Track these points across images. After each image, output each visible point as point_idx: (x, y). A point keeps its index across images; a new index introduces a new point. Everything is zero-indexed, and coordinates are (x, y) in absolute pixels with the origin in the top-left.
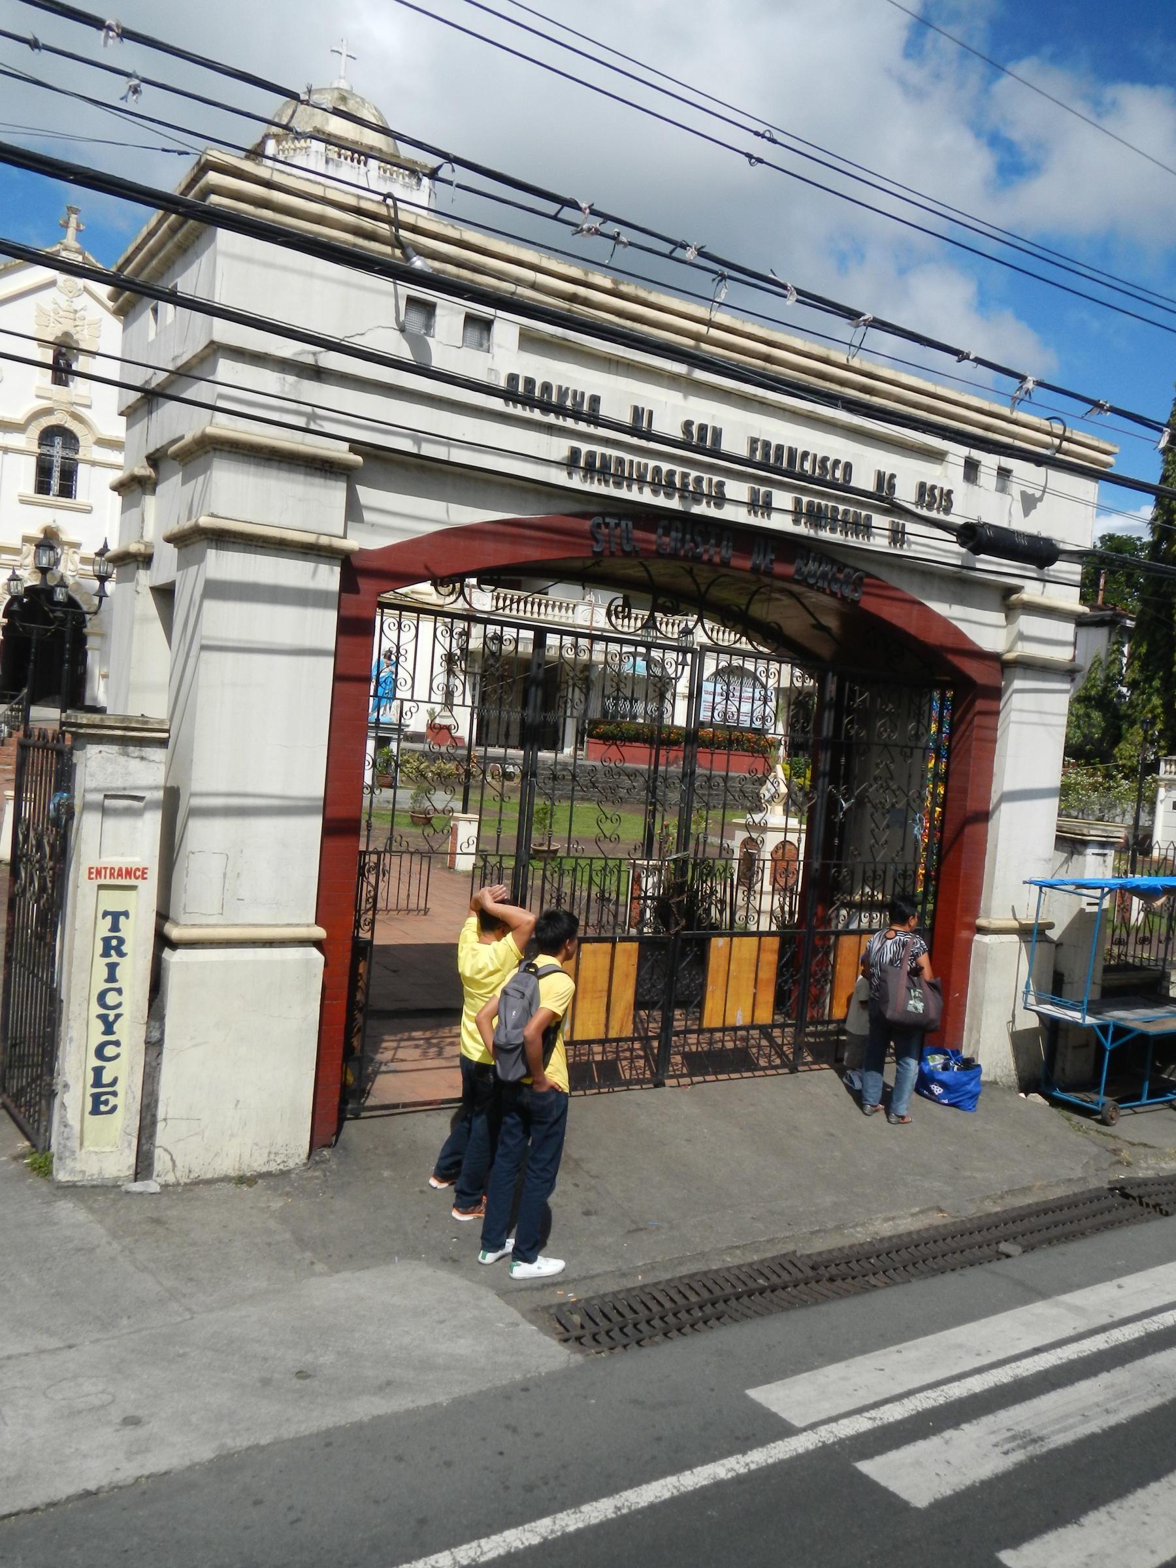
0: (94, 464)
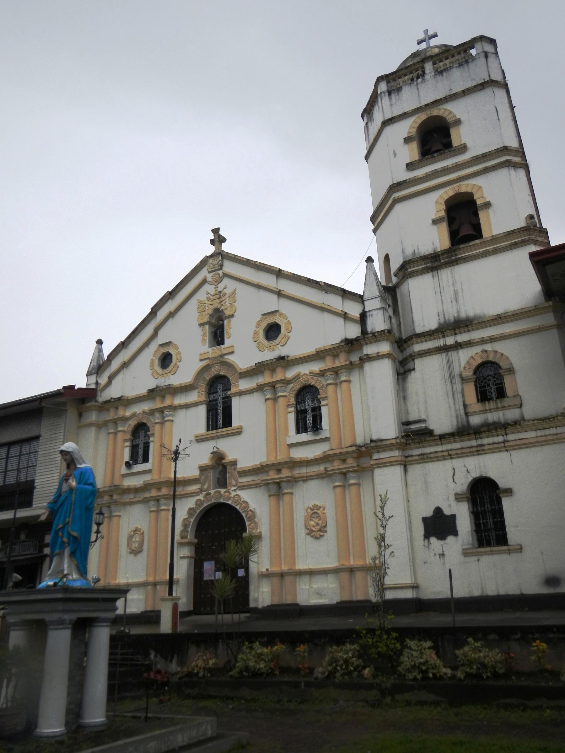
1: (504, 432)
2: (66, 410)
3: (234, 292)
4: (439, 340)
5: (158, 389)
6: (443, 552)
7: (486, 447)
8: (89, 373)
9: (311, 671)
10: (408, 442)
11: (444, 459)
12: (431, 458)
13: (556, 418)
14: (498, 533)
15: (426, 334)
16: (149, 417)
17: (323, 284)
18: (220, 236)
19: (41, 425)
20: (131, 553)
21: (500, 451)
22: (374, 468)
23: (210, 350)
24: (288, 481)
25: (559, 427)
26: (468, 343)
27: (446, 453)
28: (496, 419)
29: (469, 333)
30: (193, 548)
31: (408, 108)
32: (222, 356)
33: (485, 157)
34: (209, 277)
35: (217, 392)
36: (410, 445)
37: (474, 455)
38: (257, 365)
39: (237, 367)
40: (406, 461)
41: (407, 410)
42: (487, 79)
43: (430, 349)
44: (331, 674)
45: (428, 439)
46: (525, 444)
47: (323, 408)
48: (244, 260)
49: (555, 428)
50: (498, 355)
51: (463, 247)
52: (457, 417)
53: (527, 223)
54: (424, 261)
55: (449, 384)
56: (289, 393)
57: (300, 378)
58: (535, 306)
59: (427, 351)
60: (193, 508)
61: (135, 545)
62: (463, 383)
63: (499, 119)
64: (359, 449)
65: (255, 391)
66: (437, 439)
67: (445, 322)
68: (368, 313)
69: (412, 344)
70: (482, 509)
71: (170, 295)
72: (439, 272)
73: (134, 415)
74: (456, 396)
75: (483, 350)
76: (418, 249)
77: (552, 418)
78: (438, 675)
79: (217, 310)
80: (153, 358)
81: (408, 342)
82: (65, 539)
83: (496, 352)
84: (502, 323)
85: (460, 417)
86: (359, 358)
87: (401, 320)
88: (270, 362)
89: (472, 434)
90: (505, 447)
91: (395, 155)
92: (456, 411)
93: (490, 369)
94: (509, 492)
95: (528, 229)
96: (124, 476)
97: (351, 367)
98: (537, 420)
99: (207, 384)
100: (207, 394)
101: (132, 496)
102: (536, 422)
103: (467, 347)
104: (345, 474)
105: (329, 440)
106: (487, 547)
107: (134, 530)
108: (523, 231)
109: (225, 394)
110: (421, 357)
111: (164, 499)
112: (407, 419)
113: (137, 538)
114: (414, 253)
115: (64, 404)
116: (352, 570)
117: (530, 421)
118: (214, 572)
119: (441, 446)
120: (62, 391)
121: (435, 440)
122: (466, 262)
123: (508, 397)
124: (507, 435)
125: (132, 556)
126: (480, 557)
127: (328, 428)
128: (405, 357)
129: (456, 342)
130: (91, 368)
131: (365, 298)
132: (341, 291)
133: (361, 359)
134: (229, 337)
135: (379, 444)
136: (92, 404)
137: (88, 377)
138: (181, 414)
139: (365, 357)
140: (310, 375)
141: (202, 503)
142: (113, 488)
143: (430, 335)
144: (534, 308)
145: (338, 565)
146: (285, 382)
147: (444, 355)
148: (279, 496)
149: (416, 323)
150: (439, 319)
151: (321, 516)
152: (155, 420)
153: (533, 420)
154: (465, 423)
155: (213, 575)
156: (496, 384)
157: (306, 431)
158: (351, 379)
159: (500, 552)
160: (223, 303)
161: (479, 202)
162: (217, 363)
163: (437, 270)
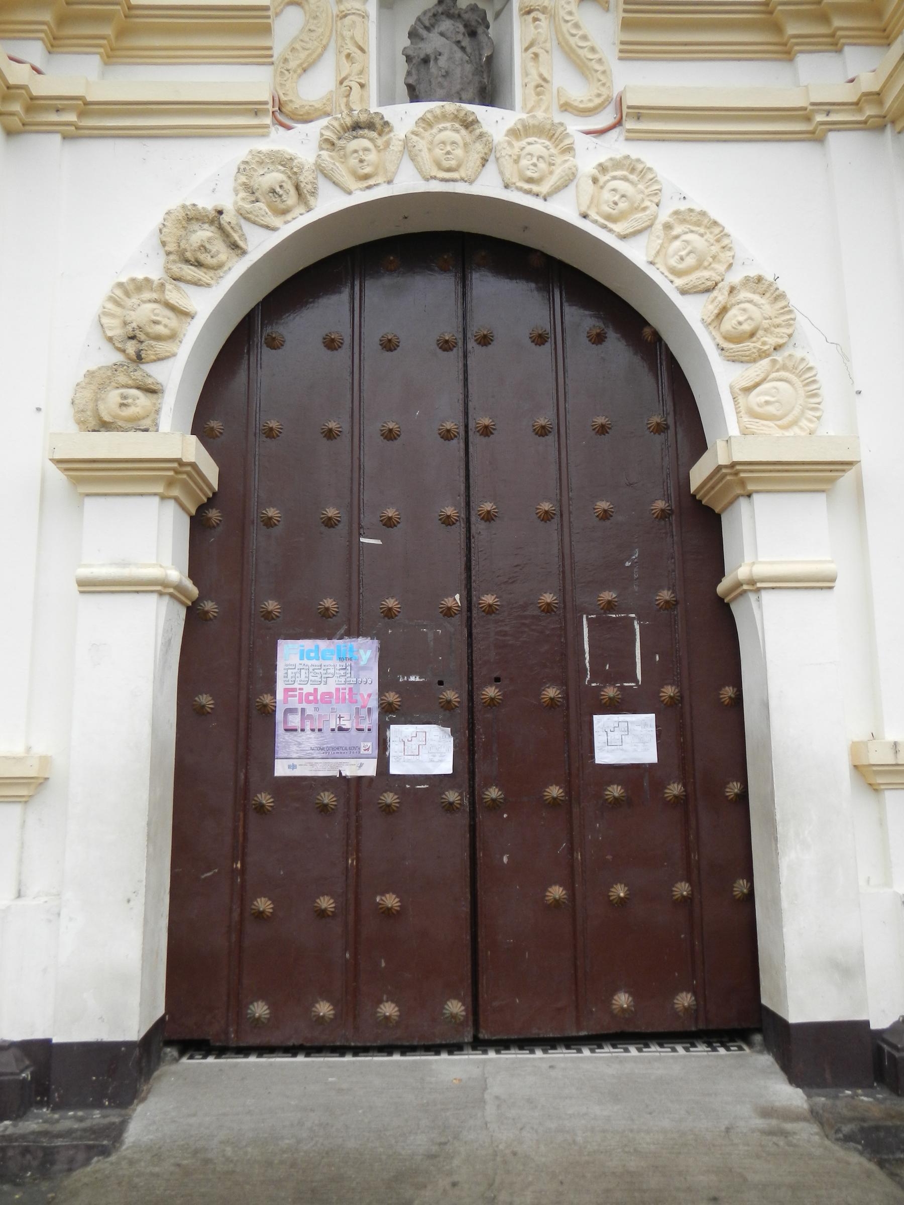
118: (375, 715)
141: (297, 187)
155: (370, 745)
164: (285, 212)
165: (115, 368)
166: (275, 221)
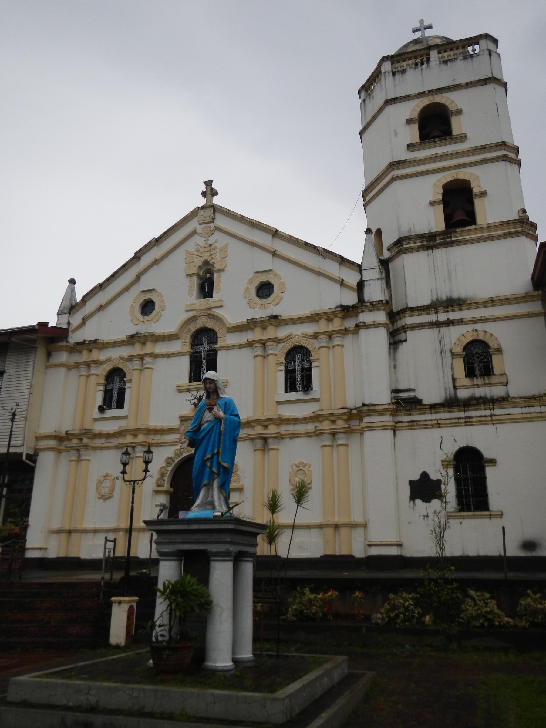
0: (228, 348)
1: (492, 406)
2: (36, 348)
3: (226, 247)
4: (431, 315)
5: (139, 335)
6: (427, 514)
7: (474, 419)
8: (60, 312)
9: (368, 618)
10: (399, 409)
11: (433, 428)
12: (420, 425)
13: (541, 398)
14: (478, 499)
15: (419, 308)
16: (126, 362)
17: (321, 249)
18: (212, 189)
19: (5, 361)
20: (99, 498)
21: (487, 424)
22: (365, 431)
23: (197, 302)
24: (275, 438)
25: (543, 406)
26: (460, 321)
27: (435, 422)
28: (483, 395)
29: (460, 311)
30: (169, 497)
31: (413, 91)
32: (209, 309)
33: (484, 148)
34: (200, 229)
35: (201, 344)
36: (401, 412)
37: (461, 426)
38: (248, 321)
39: (225, 322)
40: (395, 427)
41: (397, 378)
42: (490, 76)
43: (422, 323)
44: (392, 621)
45: (418, 407)
46: (511, 419)
47: (313, 369)
48: (238, 216)
49: (539, 407)
50: (488, 335)
51: (459, 231)
52: (445, 389)
53: (519, 216)
54: (420, 239)
55: (439, 358)
56: (280, 352)
57: (291, 338)
58: (526, 293)
59: (420, 325)
60: (172, 457)
61: (105, 491)
62: (453, 358)
63: (498, 115)
64: (350, 412)
65: (243, 347)
66: (428, 408)
67: (437, 299)
68: (366, 282)
69: (405, 317)
70: (465, 476)
71: (157, 241)
72: (434, 251)
73: (109, 360)
74: (445, 369)
75: (474, 329)
76: (414, 227)
77: (537, 397)
78: (502, 624)
79: (206, 263)
80: (134, 304)
81: (401, 314)
82: (215, 470)
83: (486, 332)
84: (493, 306)
85: (448, 390)
86: (355, 324)
87: (393, 293)
88: (262, 319)
89: (461, 406)
90: (492, 420)
91: (396, 135)
92: (445, 384)
93: (479, 347)
94: (493, 462)
95: (522, 222)
96: (96, 420)
97: (346, 332)
98: (524, 398)
99: (192, 336)
100: (191, 345)
101: (103, 440)
102: (522, 400)
103: (458, 325)
104: (334, 435)
105: (319, 401)
106: (467, 511)
107: (105, 475)
108: (517, 222)
109: (211, 347)
110: (413, 330)
111: (140, 446)
112: (397, 387)
113: (108, 483)
114: (410, 230)
115: (34, 341)
116: (336, 527)
117: (517, 399)
119: (430, 415)
120: (37, 327)
121: (425, 409)
122: (460, 245)
123: (495, 375)
124: (494, 410)
125: (101, 501)
126: (462, 520)
127: (319, 389)
128: (396, 328)
129: (448, 319)
130: (62, 308)
131: (362, 268)
132: (340, 258)
133: (357, 326)
134: (218, 291)
135: (372, 408)
136: (63, 344)
137: (59, 316)
138: (161, 363)
139: (361, 324)
140: (303, 337)
141: (181, 453)
142: (84, 431)
143: (424, 310)
144: (524, 295)
145: (322, 521)
146: (277, 341)
147: (436, 329)
148: (264, 451)
149: (409, 297)
150: (432, 296)
151: (307, 473)
152: (133, 366)
153: (520, 398)
154: (453, 396)
156: (484, 362)
157: (295, 390)
158: (344, 344)
159: (482, 517)
160: (213, 256)
161: (475, 190)
162: (204, 316)
163: (433, 249)
164: (179, 456)
165: (160, 478)
166: (178, 458)
